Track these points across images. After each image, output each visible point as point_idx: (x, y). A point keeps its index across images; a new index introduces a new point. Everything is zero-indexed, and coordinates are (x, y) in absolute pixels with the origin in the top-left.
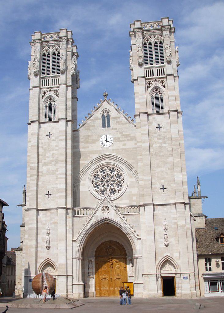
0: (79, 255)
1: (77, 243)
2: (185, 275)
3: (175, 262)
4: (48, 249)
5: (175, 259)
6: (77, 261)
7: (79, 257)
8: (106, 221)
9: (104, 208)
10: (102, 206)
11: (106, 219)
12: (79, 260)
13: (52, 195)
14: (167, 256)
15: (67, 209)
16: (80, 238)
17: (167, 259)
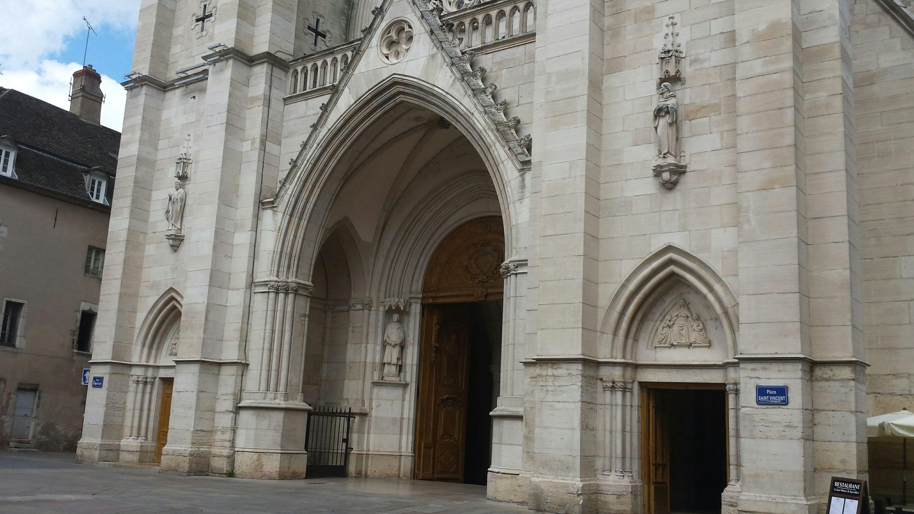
0: (284, 269)
1: (280, 215)
2: (773, 377)
3: (717, 287)
4: (175, 248)
5: (718, 268)
6: (272, 295)
7: (283, 278)
8: (401, 98)
9: (393, 34)
10: (383, 25)
11: (395, 83)
12: (281, 296)
13: (212, 18)
14: (669, 248)
15: (251, 61)
16: (289, 192)
17: (673, 274)
